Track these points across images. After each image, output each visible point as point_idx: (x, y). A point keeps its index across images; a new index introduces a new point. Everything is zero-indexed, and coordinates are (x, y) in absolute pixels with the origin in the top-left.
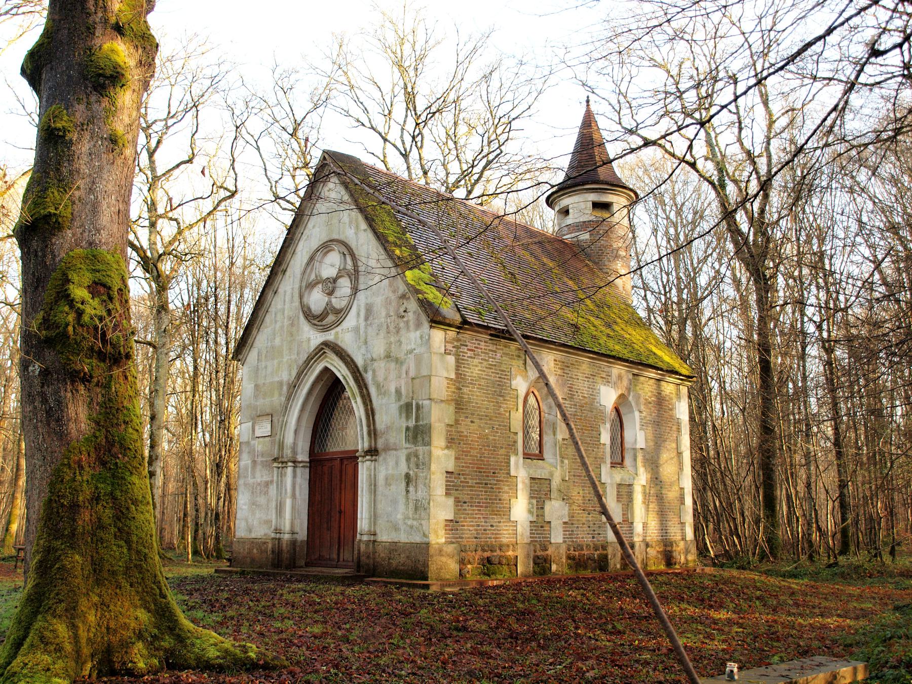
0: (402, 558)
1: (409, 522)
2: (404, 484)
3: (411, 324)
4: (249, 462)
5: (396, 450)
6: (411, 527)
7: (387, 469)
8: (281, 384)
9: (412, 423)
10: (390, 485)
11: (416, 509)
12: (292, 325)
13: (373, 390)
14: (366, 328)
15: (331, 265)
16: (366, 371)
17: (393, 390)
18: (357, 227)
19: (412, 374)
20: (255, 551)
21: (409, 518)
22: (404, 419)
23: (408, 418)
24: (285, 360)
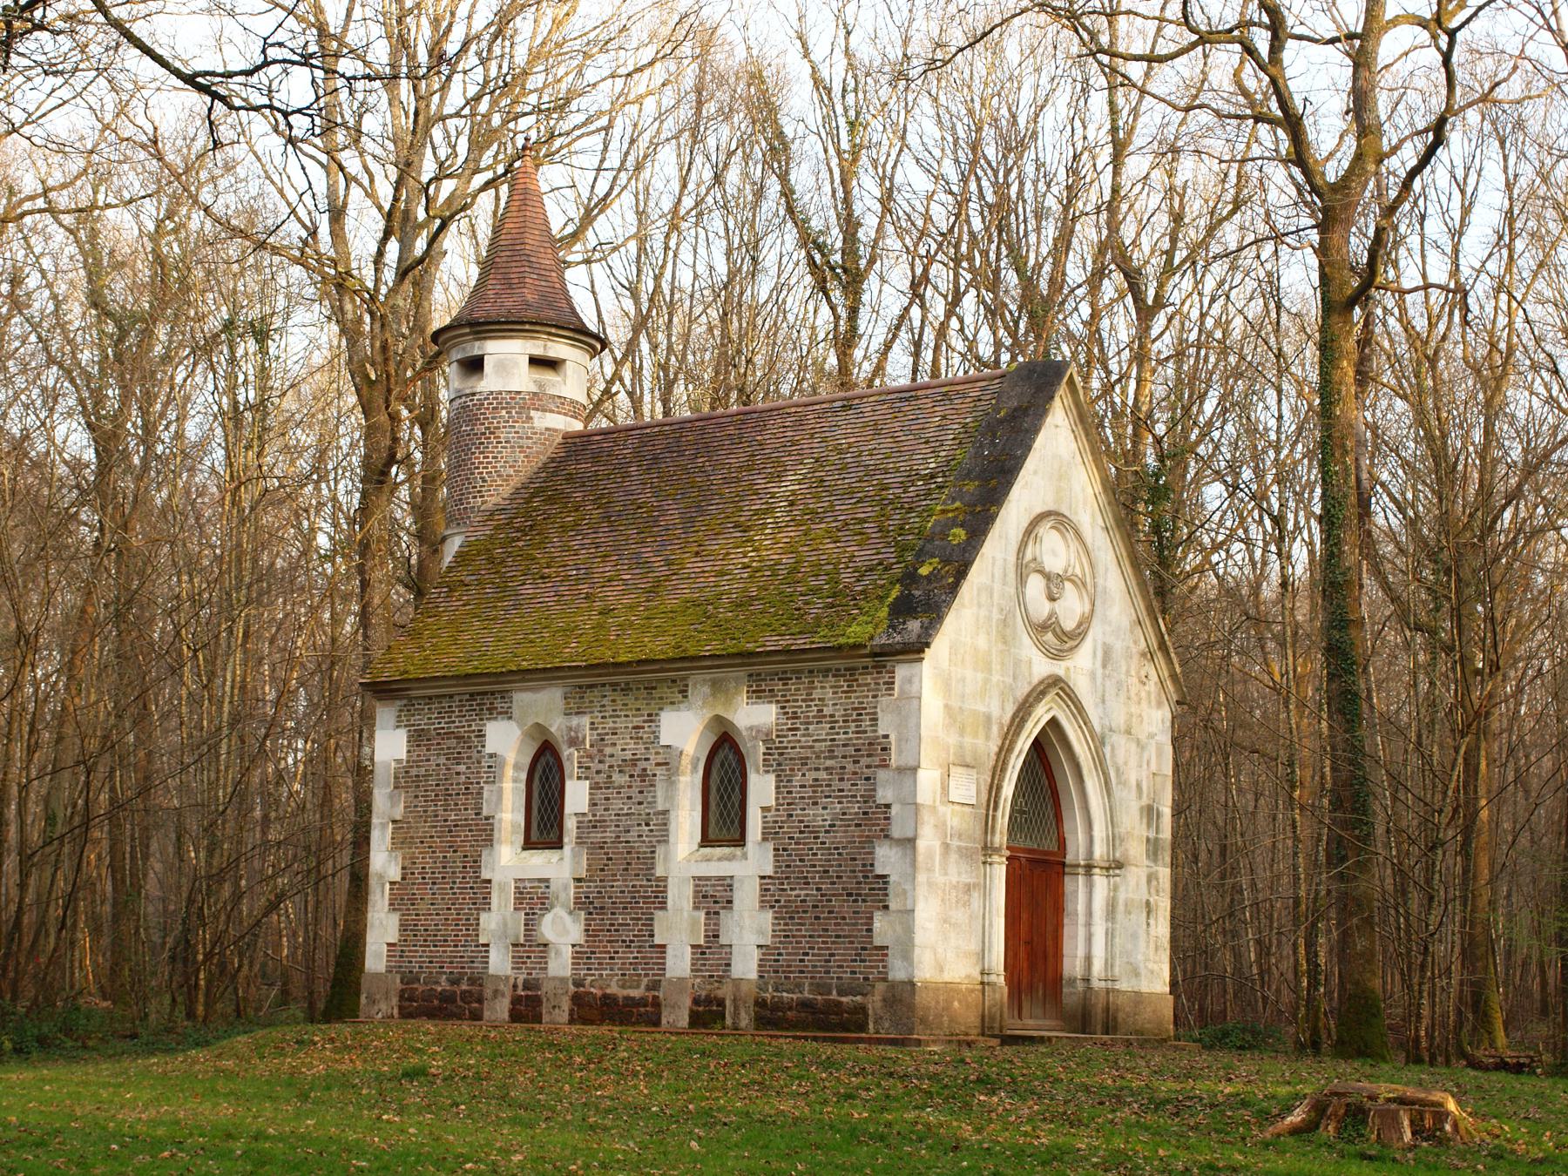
2: (1145, 914)
4: (937, 844)
9: (1152, 835)
11: (1157, 949)
12: (1005, 622)
15: (1054, 551)
17: (1134, 783)
19: (1153, 768)
20: (956, 1004)
22: (1144, 826)
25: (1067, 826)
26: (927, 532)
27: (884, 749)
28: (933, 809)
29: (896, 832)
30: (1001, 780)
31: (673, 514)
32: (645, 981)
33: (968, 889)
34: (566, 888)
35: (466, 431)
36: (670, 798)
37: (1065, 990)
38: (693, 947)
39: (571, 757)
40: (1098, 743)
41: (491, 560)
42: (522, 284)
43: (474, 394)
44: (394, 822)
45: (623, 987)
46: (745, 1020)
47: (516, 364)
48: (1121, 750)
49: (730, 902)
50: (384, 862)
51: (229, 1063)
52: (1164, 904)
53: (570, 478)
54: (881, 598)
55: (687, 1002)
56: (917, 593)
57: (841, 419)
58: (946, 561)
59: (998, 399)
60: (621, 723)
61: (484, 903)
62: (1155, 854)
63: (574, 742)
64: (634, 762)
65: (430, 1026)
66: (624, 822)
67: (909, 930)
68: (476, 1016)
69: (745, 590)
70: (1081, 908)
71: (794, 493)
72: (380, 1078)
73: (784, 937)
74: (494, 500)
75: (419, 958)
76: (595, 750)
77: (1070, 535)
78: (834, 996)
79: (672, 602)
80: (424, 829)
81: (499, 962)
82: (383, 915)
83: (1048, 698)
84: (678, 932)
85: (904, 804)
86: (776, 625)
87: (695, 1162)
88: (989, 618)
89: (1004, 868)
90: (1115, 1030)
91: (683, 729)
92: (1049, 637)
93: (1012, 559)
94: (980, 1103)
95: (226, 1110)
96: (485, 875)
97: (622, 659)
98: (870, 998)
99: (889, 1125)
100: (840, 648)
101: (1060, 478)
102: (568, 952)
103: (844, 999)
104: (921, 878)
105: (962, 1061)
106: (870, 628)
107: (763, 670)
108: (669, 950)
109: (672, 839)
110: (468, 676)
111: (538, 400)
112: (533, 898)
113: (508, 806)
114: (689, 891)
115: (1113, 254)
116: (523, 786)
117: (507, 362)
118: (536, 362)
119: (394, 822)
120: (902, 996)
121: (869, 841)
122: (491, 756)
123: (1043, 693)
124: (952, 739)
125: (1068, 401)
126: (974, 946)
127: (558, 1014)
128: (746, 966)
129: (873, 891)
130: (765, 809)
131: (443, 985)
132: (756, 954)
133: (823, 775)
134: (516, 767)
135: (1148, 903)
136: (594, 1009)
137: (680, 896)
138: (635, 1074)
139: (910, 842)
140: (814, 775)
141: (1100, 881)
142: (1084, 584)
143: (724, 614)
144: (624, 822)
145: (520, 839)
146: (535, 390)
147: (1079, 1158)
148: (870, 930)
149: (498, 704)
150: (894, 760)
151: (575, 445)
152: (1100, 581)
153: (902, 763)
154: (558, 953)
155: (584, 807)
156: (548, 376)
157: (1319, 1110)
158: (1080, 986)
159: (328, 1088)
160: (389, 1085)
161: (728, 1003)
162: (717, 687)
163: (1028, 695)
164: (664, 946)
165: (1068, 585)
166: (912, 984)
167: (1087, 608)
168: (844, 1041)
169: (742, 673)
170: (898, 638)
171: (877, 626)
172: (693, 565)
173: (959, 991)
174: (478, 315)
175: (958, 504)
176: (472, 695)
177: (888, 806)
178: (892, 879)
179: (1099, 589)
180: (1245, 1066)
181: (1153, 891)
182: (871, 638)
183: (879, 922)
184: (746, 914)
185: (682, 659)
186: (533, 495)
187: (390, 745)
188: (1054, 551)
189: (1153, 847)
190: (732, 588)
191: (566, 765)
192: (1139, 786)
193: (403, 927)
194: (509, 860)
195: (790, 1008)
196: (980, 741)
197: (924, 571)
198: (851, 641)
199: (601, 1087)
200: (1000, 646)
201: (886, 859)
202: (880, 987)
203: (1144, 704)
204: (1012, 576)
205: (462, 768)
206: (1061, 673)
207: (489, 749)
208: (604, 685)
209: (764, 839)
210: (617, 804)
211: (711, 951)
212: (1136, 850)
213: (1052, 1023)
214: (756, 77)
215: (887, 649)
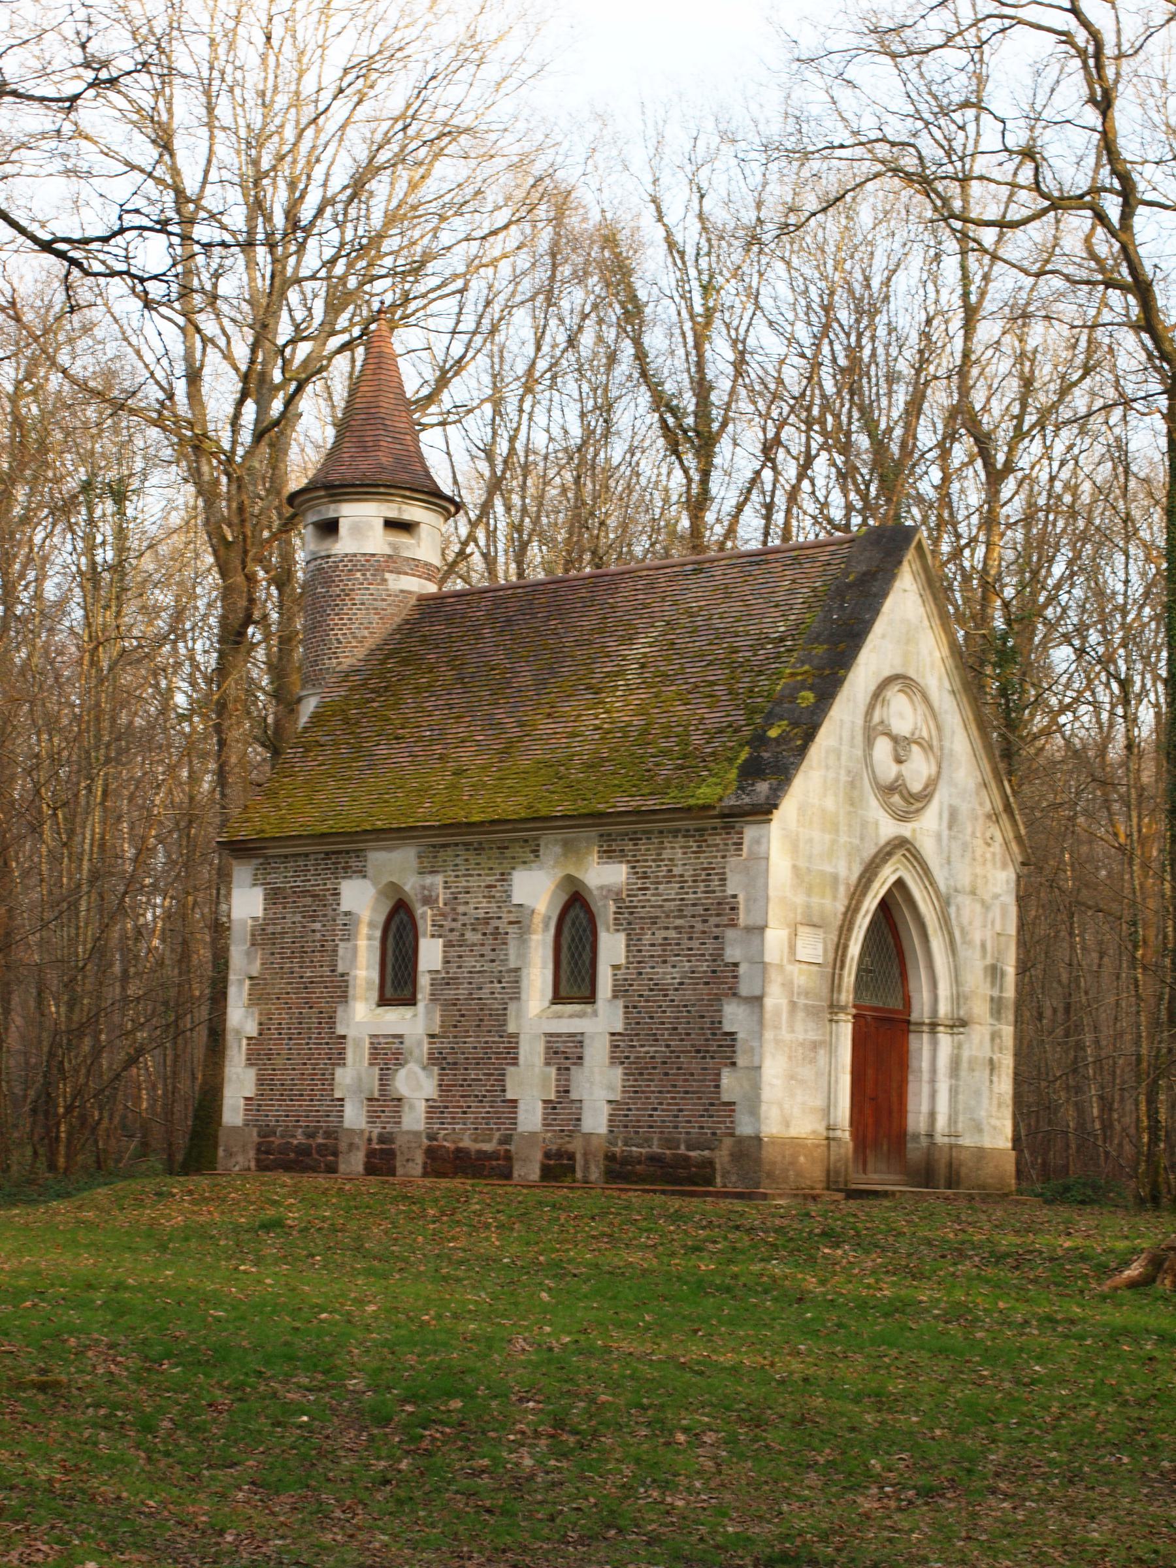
2: (987, 1072)
3: (998, 857)
4: (784, 1002)
9: (996, 994)
12: (852, 785)
15: (902, 714)
18: (940, 679)
19: (998, 928)
22: (988, 985)
23: (993, 984)
25: (912, 985)
26: (776, 695)
27: (733, 909)
28: (781, 967)
29: (744, 990)
30: (848, 939)
31: (526, 676)
32: (497, 1135)
33: (815, 1046)
34: (420, 1044)
35: (322, 593)
36: (523, 955)
37: (910, 1145)
38: (545, 1101)
39: (425, 916)
40: (944, 902)
41: (346, 720)
42: (377, 447)
43: (329, 556)
44: (251, 978)
45: (475, 1141)
46: (595, 1174)
47: (371, 527)
48: (966, 911)
49: (580, 1058)
50: (241, 1018)
51: (89, 1215)
52: (1007, 1062)
53: (424, 640)
54: (731, 760)
55: (539, 1156)
56: (766, 755)
57: (690, 583)
58: (795, 724)
59: (848, 563)
60: (473, 882)
61: (339, 1058)
62: (999, 1012)
63: (428, 901)
64: (486, 920)
65: (286, 1178)
66: (478, 979)
67: (756, 1087)
68: (332, 1169)
69: (596, 751)
70: (925, 1065)
71: (645, 655)
72: (237, 1229)
73: (633, 1091)
74: (349, 661)
75: (275, 1112)
76: (448, 909)
77: (918, 698)
78: (682, 1150)
79: (525, 763)
80: (280, 985)
81: (354, 1116)
82: (239, 1070)
83: (894, 859)
84: (529, 1088)
85: (752, 962)
86: (627, 786)
87: (545, 1313)
89: (850, 1026)
90: (958, 1186)
91: (535, 889)
92: (896, 799)
93: (860, 722)
94: (825, 1256)
95: (86, 1262)
96: (340, 1031)
97: (476, 818)
98: (717, 1153)
99: (735, 1277)
100: (689, 809)
101: (908, 642)
102: (422, 1106)
103: (692, 1154)
104: (769, 1035)
105: (808, 1215)
106: (719, 790)
107: (614, 831)
108: (522, 1106)
109: (524, 996)
110: (323, 835)
111: (393, 563)
112: (387, 1054)
113: (363, 963)
114: (540, 1047)
115: (963, 417)
116: (377, 943)
117: (362, 524)
118: (392, 525)
119: (251, 978)
120: (749, 1151)
121: (718, 999)
122: (347, 914)
123: (890, 854)
124: (800, 899)
125: (917, 565)
126: (819, 1102)
127: (413, 1166)
128: (596, 1121)
129: (722, 1048)
130: (616, 967)
131: (299, 1139)
132: (606, 1110)
133: (672, 934)
134: (371, 925)
135: (991, 1060)
136: (446, 1162)
137: (532, 1052)
138: (487, 1226)
139: (757, 1001)
140: (664, 934)
141: (945, 1040)
142: (931, 747)
143: (576, 775)
144: (478, 979)
145: (375, 995)
146: (388, 551)
147: (921, 1310)
148: (718, 1086)
149: (353, 863)
150: (743, 919)
151: (429, 607)
152: (947, 744)
153: (750, 922)
154: (412, 1107)
155: (438, 966)
156: (403, 539)
157: (1157, 1264)
158: (924, 1142)
159: (186, 1239)
160: (247, 1236)
161: (579, 1157)
162: (569, 847)
163: (875, 856)
164: (515, 1101)
165: (915, 748)
166: (758, 1139)
167: (934, 770)
168: (692, 1194)
169: (593, 833)
170: (747, 800)
171: (726, 788)
172: (545, 726)
173: (805, 1146)
174: (334, 477)
175: (806, 667)
176: (327, 854)
177: (736, 965)
178: (740, 1036)
179: (946, 751)
180: (1085, 1221)
182: (721, 799)
183: (727, 1079)
184: (596, 1070)
185: (534, 819)
186: (388, 657)
187: (247, 903)
189: (997, 1006)
190: (583, 749)
191: (420, 923)
192: (983, 946)
193: (260, 1082)
194: (363, 1017)
195: (639, 1163)
196: (827, 902)
197: (773, 733)
198: (701, 802)
199: (454, 1239)
201: (734, 1016)
202: (728, 1142)
203: (989, 865)
205: (317, 926)
206: (907, 834)
207: (344, 907)
208: (457, 845)
209: (615, 997)
210: (470, 962)
211: (562, 1105)
212: (980, 1009)
213: (896, 1178)
214: (610, 240)
215: (736, 811)
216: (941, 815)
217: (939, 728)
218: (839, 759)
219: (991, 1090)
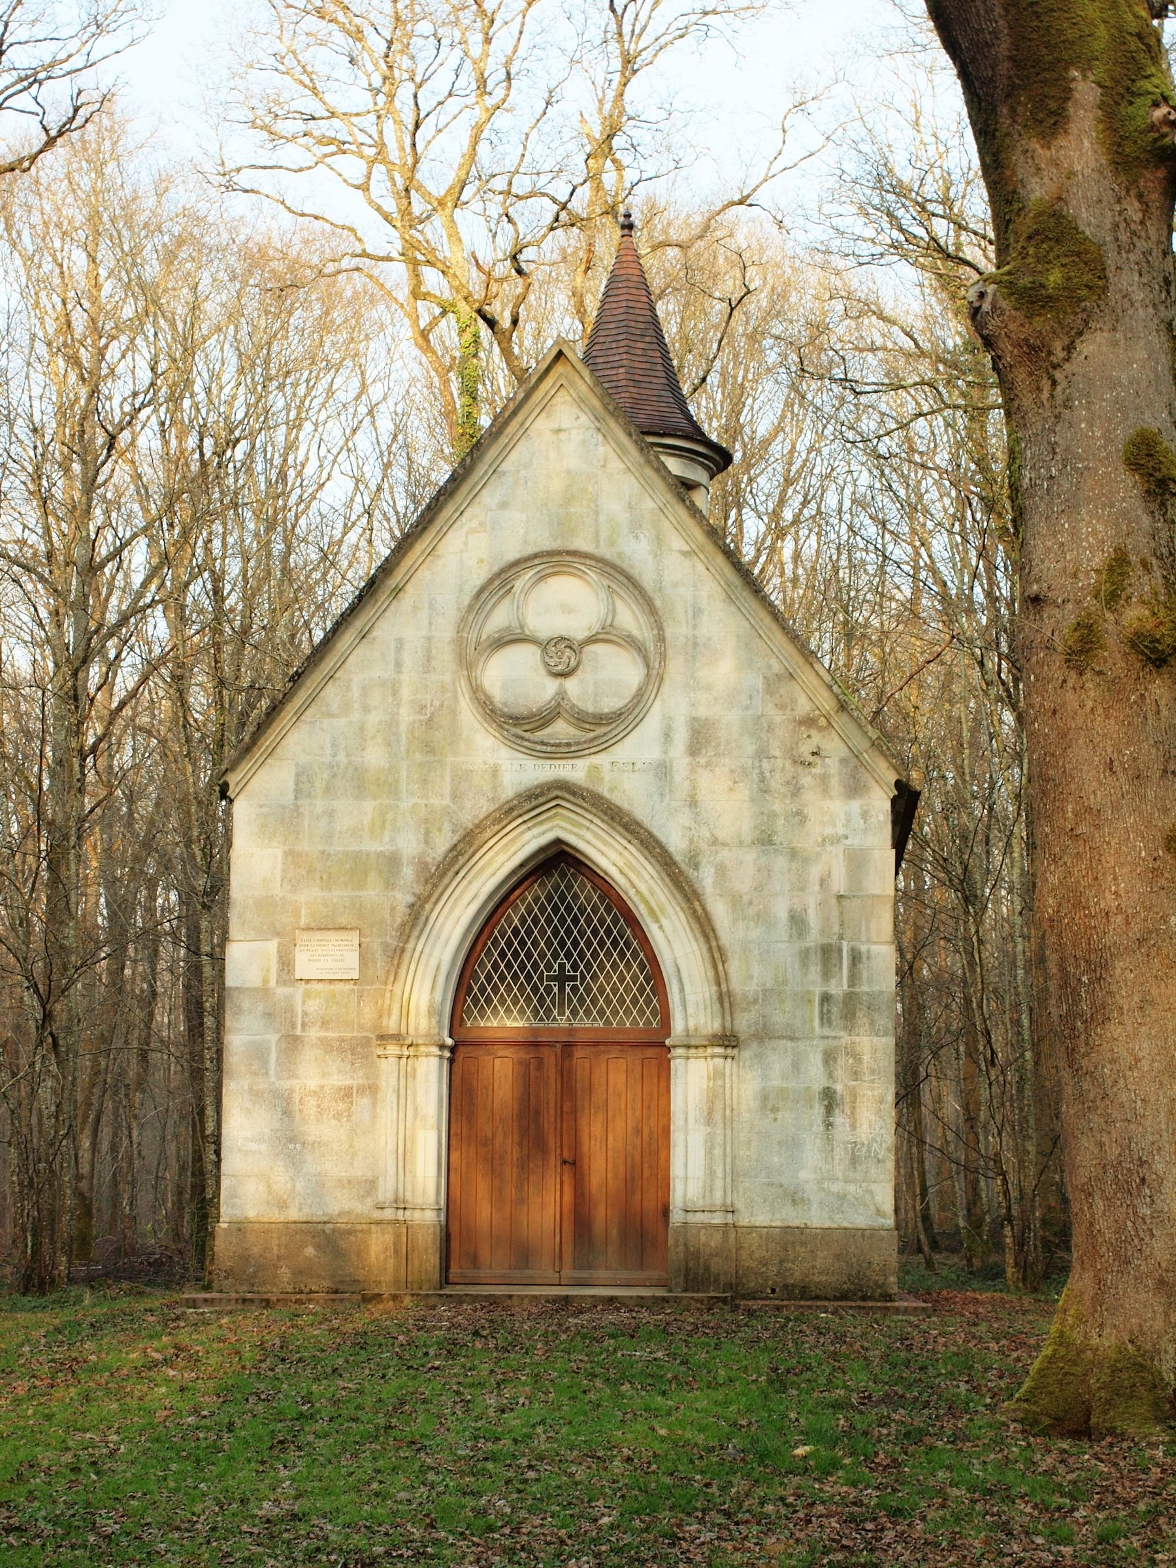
0: (823, 1259)
1: (835, 1188)
2: (818, 1111)
3: (834, 782)
4: (273, 1038)
5: (792, 1039)
6: (842, 1197)
7: (765, 1077)
8: (392, 861)
9: (839, 987)
10: (775, 1110)
11: (854, 1161)
12: (430, 724)
13: (719, 911)
14: (693, 770)
15: (565, 605)
16: (696, 866)
18: (659, 540)
19: (839, 883)
20: (310, 1251)
21: (834, 1179)
23: (826, 975)
24: (405, 804)
33: (347, 1094)
88: (392, 724)
93: (445, 631)
152: (677, 631)
181: (839, 1073)
188: (565, 605)
192: (797, 922)
200: (419, 757)
204: (445, 657)
216: (667, 736)
217: (651, 609)
218: (395, 693)
219: (829, 1140)
